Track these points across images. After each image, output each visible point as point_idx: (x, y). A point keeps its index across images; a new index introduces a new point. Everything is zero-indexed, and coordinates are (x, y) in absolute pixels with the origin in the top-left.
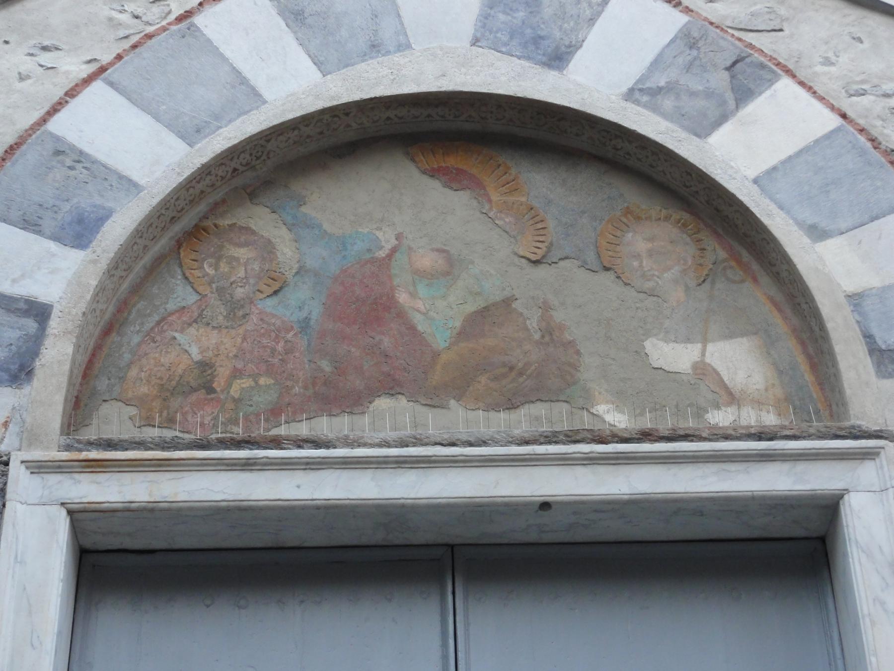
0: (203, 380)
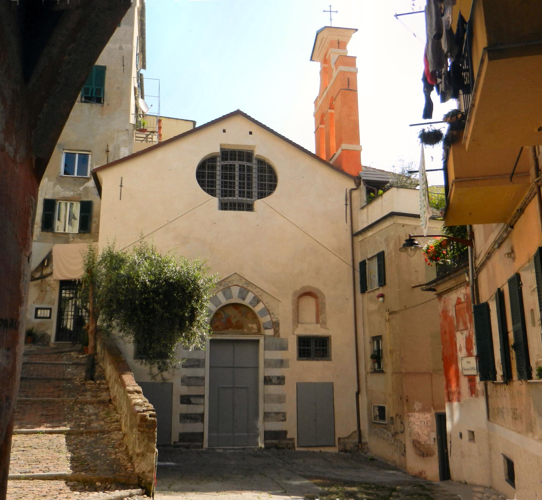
0: (217, 327)
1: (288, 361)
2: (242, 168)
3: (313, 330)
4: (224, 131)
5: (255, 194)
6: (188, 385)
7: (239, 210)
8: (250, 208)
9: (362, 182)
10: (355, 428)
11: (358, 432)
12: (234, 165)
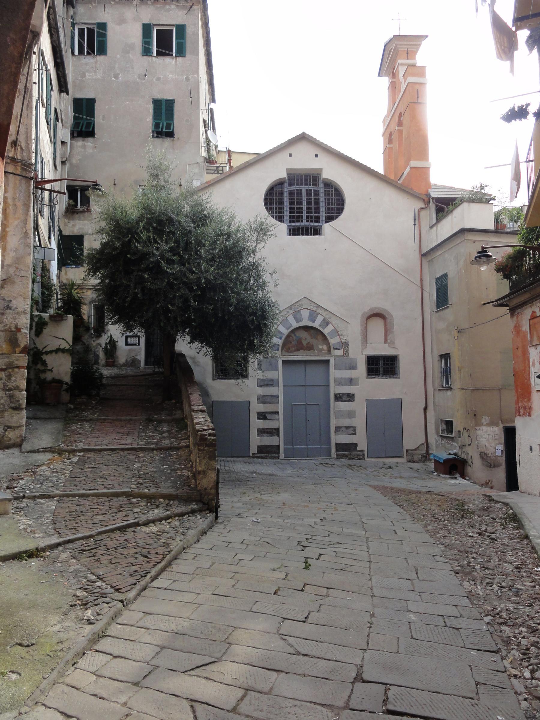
1: (357, 379)
2: (309, 192)
3: (380, 349)
4: (290, 155)
5: (323, 218)
6: (264, 403)
7: (307, 235)
8: (317, 232)
9: (431, 200)
10: (423, 441)
11: (425, 444)
12: (301, 190)
